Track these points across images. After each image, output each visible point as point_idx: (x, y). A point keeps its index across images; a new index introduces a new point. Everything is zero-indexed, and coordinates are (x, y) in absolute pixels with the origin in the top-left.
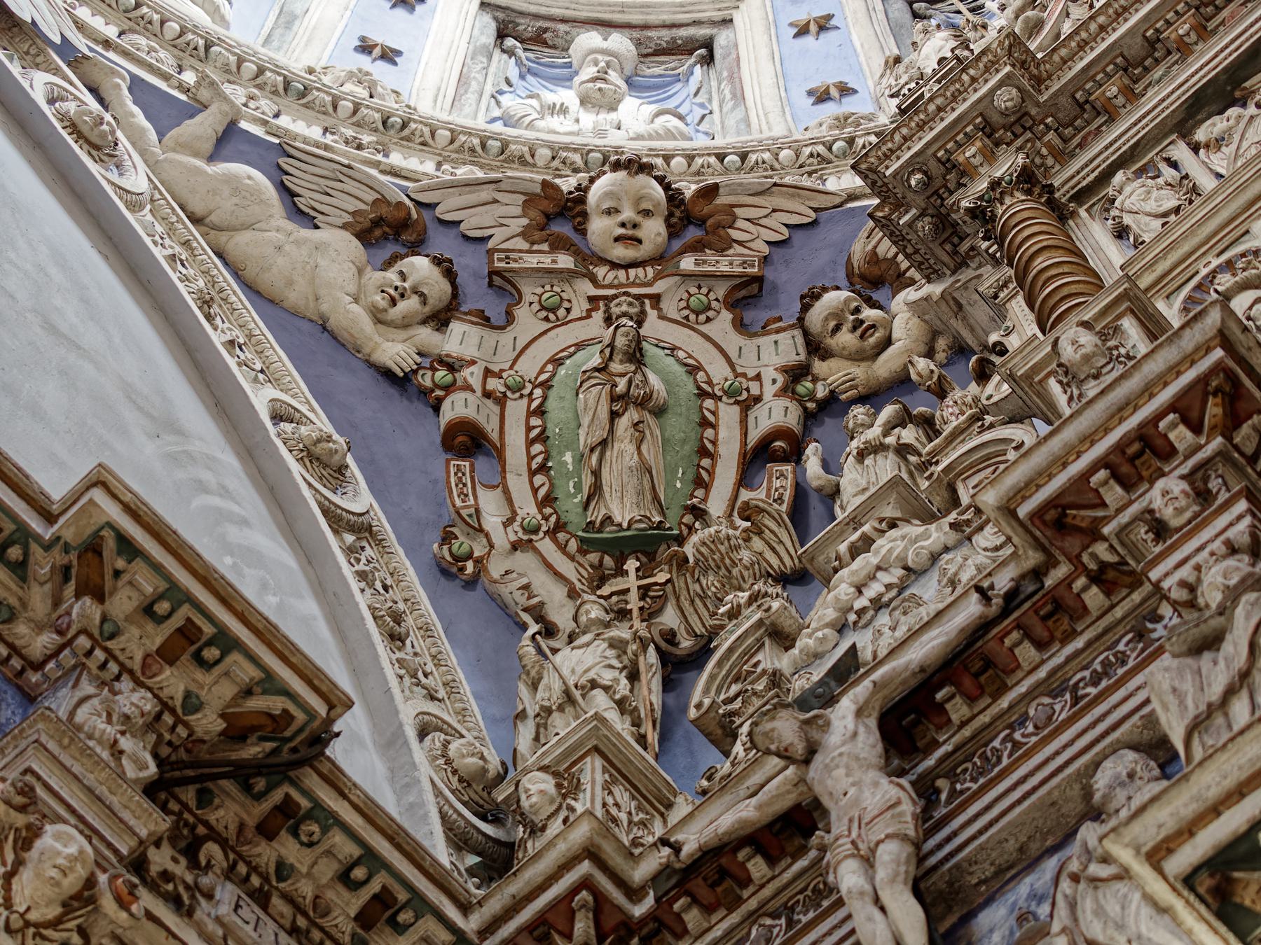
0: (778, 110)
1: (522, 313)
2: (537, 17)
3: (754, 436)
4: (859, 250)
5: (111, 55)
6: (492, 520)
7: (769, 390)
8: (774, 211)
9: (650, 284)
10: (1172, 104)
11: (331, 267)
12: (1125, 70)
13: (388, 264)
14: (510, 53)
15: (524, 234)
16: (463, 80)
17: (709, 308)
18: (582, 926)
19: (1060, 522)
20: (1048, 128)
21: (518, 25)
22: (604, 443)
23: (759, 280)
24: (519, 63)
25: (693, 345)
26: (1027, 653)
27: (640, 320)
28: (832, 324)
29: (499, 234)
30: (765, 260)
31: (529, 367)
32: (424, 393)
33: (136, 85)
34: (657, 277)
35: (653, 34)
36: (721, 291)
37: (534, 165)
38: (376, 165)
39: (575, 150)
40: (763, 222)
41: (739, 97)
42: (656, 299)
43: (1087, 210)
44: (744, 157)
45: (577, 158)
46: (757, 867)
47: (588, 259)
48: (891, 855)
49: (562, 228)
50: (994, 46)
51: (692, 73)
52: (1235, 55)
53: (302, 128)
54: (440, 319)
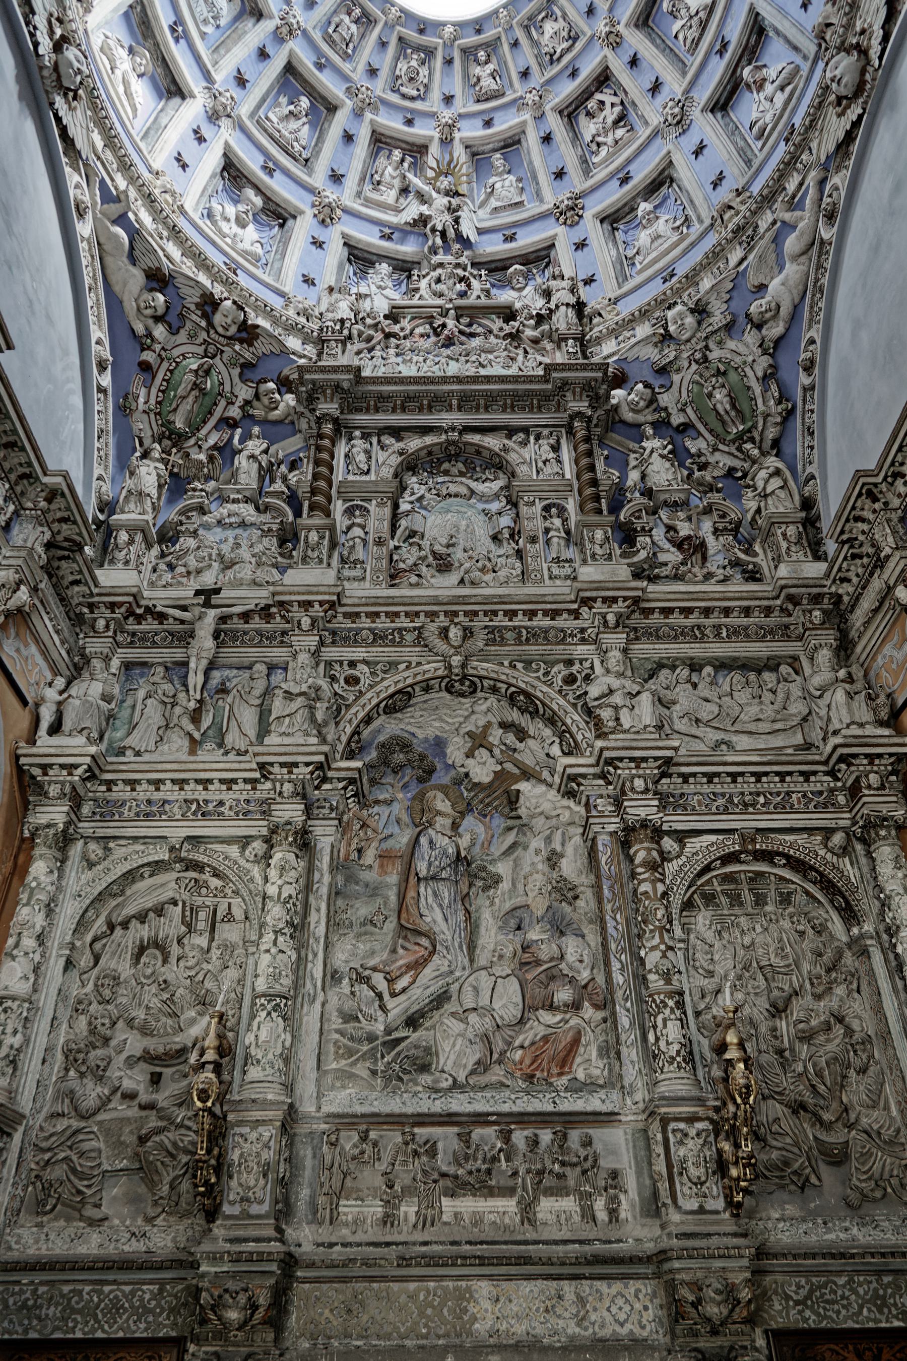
1: (183, 332)
3: (226, 414)
4: (286, 372)
5: (98, 164)
6: (141, 400)
7: (238, 404)
11: (132, 280)
13: (151, 290)
15: (197, 305)
18: (123, 610)
19: (281, 604)
22: (184, 398)
23: (254, 366)
25: (223, 373)
26: (257, 619)
27: (213, 357)
29: (189, 299)
30: (259, 358)
31: (176, 352)
32: (142, 344)
33: (102, 181)
36: (242, 361)
38: (163, 250)
41: (283, 256)
46: (171, 620)
47: (210, 324)
48: (204, 663)
49: (208, 309)
53: (146, 218)
54: (157, 319)
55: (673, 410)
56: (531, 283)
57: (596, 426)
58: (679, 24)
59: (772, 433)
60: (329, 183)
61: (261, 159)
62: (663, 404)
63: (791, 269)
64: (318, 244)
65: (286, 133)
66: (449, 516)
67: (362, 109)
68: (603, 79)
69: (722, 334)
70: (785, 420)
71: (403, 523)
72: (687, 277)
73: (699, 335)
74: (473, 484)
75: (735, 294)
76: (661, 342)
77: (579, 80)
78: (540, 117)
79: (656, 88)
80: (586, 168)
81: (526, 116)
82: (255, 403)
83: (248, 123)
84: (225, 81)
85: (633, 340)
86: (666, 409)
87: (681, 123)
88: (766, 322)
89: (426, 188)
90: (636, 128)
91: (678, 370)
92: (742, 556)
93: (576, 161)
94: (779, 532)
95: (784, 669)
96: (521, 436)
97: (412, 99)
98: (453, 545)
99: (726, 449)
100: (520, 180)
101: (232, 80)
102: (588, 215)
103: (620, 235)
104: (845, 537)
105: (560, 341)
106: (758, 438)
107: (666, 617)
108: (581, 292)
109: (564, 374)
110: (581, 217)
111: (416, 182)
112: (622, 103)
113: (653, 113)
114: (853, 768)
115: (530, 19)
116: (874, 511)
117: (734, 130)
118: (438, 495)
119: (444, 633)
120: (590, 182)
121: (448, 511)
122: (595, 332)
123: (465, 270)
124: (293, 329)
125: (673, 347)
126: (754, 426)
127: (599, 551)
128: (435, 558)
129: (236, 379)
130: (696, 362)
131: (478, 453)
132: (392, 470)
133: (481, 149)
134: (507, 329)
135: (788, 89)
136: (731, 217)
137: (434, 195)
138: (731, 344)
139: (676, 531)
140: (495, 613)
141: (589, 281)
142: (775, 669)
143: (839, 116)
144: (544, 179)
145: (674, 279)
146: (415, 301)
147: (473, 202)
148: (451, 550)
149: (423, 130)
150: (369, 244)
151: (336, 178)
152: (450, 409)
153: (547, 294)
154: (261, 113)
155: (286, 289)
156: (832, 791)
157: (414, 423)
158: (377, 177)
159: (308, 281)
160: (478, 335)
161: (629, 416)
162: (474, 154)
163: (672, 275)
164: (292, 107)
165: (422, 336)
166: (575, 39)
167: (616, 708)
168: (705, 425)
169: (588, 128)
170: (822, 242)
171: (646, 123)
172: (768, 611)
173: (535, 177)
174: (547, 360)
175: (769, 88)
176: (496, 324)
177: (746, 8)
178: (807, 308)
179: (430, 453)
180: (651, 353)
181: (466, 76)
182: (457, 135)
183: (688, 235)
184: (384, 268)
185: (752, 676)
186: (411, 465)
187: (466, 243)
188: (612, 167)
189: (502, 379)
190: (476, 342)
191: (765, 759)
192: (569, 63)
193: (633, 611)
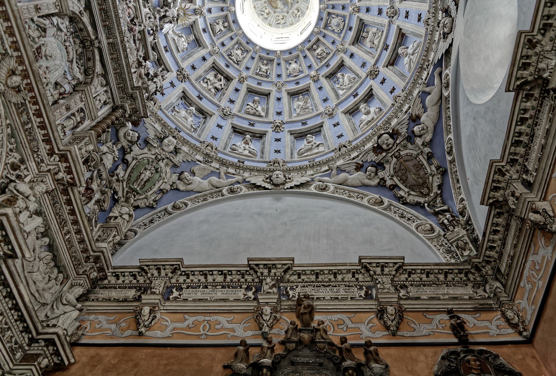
55: (132, 154)
58: (252, 105)
59: (141, 203)
62: (133, 148)
63: (205, 183)
66: (59, 51)
68: (228, 79)
69: (171, 164)
70: (148, 207)
71: (47, 22)
72: (184, 139)
73: (167, 154)
74: (75, 60)
75: (187, 163)
76: (158, 138)
77: (225, 68)
78: (210, 54)
79: (232, 102)
81: (210, 48)
85: (153, 124)
86: (131, 151)
87: (225, 115)
88: (182, 181)
91: (149, 150)
92: (94, 221)
93: (199, 74)
94: (114, 233)
95: (61, 276)
96: (104, 83)
98: (47, 59)
99: (125, 186)
102: (183, 85)
103: (180, 102)
104: (146, 268)
105: (147, 89)
106: (136, 198)
107: (65, 204)
109: (139, 97)
110: (182, 82)
114: (45, 349)
115: (240, 43)
116: (166, 275)
117: (229, 138)
118: (65, 41)
119: (13, 73)
120: (194, 82)
121: (61, 50)
126: (140, 195)
127: (83, 151)
128: (37, 49)
130: (156, 157)
131: (89, 59)
132: (71, 9)
133: (194, 28)
134: (141, 60)
135: (250, 155)
136: (209, 150)
137: (177, 9)
138: (168, 169)
139: (91, 182)
140: (36, 103)
141: (163, 94)
142: (60, 272)
143: (263, 181)
144: (190, 61)
146: (142, 7)
148: (44, 58)
152: (108, 38)
153: (156, 75)
156: (21, 347)
157: (96, 18)
160: (136, 45)
161: (121, 133)
162: (192, 26)
165: (129, 13)
166: (238, 64)
167: (27, 208)
168: (131, 172)
169: (211, 76)
170: (221, 191)
172: (85, 251)
173: (190, 56)
175: (247, 147)
176: (141, 53)
177: (266, 129)
178: (195, 196)
179: (81, 30)
181: (218, 18)
182: (198, 17)
185: (52, 264)
186: (73, 19)
188: (202, 90)
191: (29, 304)
192: (230, 63)
193: (64, 185)
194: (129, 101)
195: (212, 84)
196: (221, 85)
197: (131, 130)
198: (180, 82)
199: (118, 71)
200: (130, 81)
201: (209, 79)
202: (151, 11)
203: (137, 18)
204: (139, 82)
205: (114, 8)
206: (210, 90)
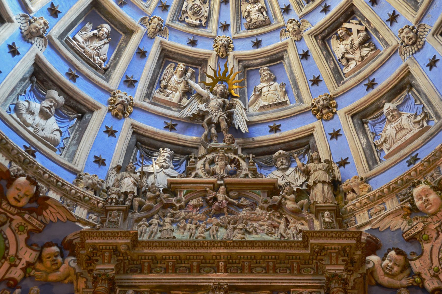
0: (84, 158)
2: (46, 76)
4: (70, 237)
7: (20, 266)
8: (58, 213)
9: (13, 215)
10: (155, 282)
12: (153, 260)
14: (32, 81)
16: (14, 89)
17: (23, 231)
20: (128, 259)
21: (40, 75)
23: (40, 231)
24: (32, 87)
28: (48, 256)
34: (17, 214)
35: (72, 101)
36: (30, 227)
37: (10, 153)
39: (23, 156)
40: (53, 214)
42: (12, 220)
43: (119, 291)
44: (63, 185)
45: (22, 159)
50: (131, 232)
51: (73, 120)
52: (174, 284)
55: (426, 276)
56: (294, 165)
57: (353, 288)
60: (123, 86)
61: (66, 68)
64: (111, 132)
65: (90, 50)
67: (154, 34)
72: (428, 161)
77: (329, 14)
79: (393, 18)
80: (338, 77)
82: (39, 266)
83: (58, 42)
84: (41, 11)
85: (384, 213)
86: (419, 275)
89: (205, 92)
90: (379, 48)
91: (428, 240)
97: (196, 26)
100: (283, 85)
101: (46, 10)
102: (341, 112)
105: (318, 211)
108: (336, 171)
111: (197, 87)
112: (366, 30)
113: (391, 36)
120: (342, 88)
122: (349, 206)
123: (236, 153)
124: (79, 200)
125: (420, 219)
129: (22, 244)
137: (211, 96)
141: (343, 163)
145: (418, 163)
147: (244, 102)
149: (201, 49)
150: (154, 133)
151: (130, 83)
152: (216, 270)
153: (307, 173)
154: (70, 35)
155: (79, 168)
158: (164, 83)
159: (99, 161)
160: (246, 206)
163: (416, 159)
164: (95, 32)
165: (195, 206)
169: (338, 48)
171: (387, 44)
173: (296, 84)
174: (306, 228)
180: (399, 223)
183: (428, 128)
184: (166, 152)
187: (237, 132)
189: (265, 244)
190: (243, 213)
194: (325, 258)
195: (354, 51)
196: (359, 31)
197: (383, 260)
198: (336, 116)
199: (271, 264)
200: (291, 247)
201: (344, 55)
202: (203, 156)
203: (206, 191)
204: (304, 219)
205: (175, 247)
206: (363, 58)
